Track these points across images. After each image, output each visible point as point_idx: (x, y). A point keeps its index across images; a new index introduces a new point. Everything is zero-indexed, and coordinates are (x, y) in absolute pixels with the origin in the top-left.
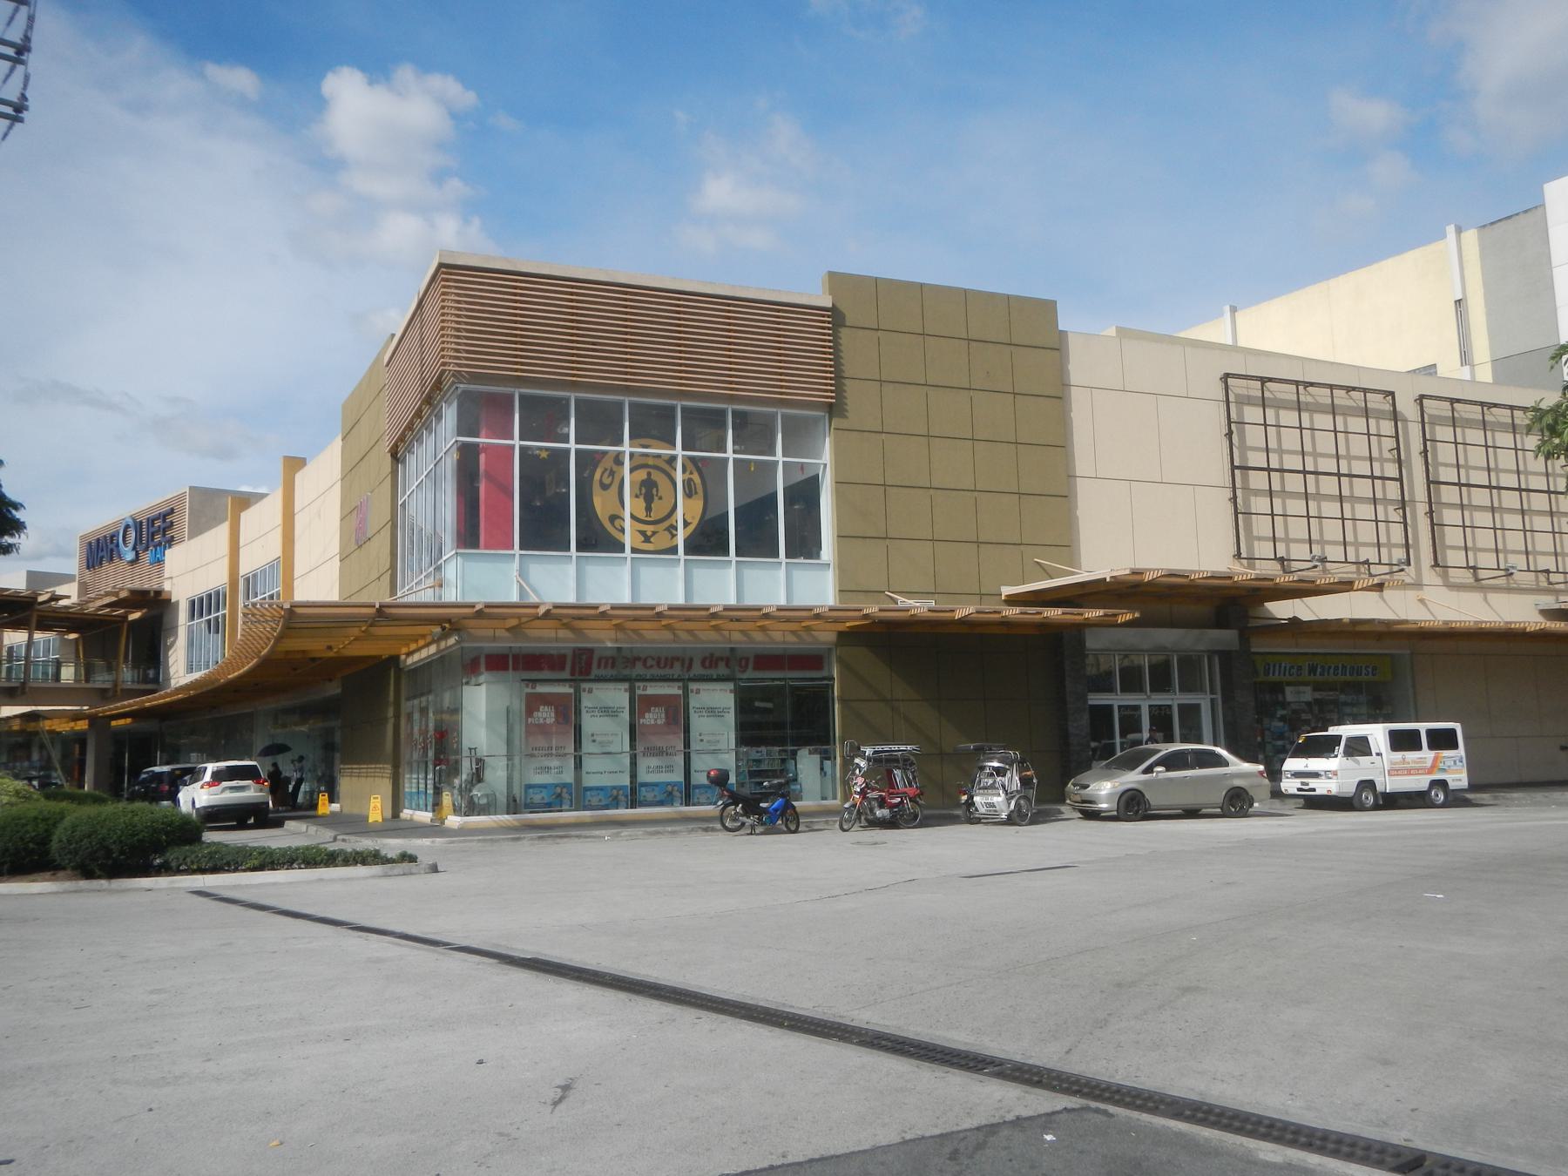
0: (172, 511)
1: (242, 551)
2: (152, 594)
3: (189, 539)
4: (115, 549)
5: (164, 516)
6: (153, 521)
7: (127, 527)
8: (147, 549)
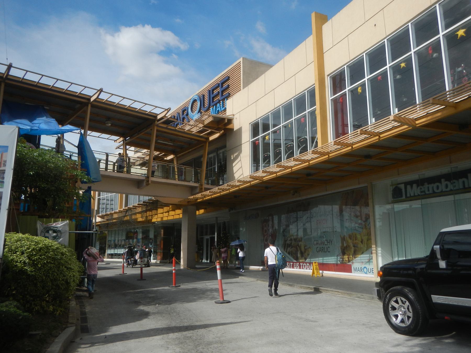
0: (228, 79)
1: (325, 55)
2: (226, 121)
3: (243, 89)
4: (186, 117)
5: (223, 84)
6: (213, 90)
7: (195, 101)
8: (208, 109)
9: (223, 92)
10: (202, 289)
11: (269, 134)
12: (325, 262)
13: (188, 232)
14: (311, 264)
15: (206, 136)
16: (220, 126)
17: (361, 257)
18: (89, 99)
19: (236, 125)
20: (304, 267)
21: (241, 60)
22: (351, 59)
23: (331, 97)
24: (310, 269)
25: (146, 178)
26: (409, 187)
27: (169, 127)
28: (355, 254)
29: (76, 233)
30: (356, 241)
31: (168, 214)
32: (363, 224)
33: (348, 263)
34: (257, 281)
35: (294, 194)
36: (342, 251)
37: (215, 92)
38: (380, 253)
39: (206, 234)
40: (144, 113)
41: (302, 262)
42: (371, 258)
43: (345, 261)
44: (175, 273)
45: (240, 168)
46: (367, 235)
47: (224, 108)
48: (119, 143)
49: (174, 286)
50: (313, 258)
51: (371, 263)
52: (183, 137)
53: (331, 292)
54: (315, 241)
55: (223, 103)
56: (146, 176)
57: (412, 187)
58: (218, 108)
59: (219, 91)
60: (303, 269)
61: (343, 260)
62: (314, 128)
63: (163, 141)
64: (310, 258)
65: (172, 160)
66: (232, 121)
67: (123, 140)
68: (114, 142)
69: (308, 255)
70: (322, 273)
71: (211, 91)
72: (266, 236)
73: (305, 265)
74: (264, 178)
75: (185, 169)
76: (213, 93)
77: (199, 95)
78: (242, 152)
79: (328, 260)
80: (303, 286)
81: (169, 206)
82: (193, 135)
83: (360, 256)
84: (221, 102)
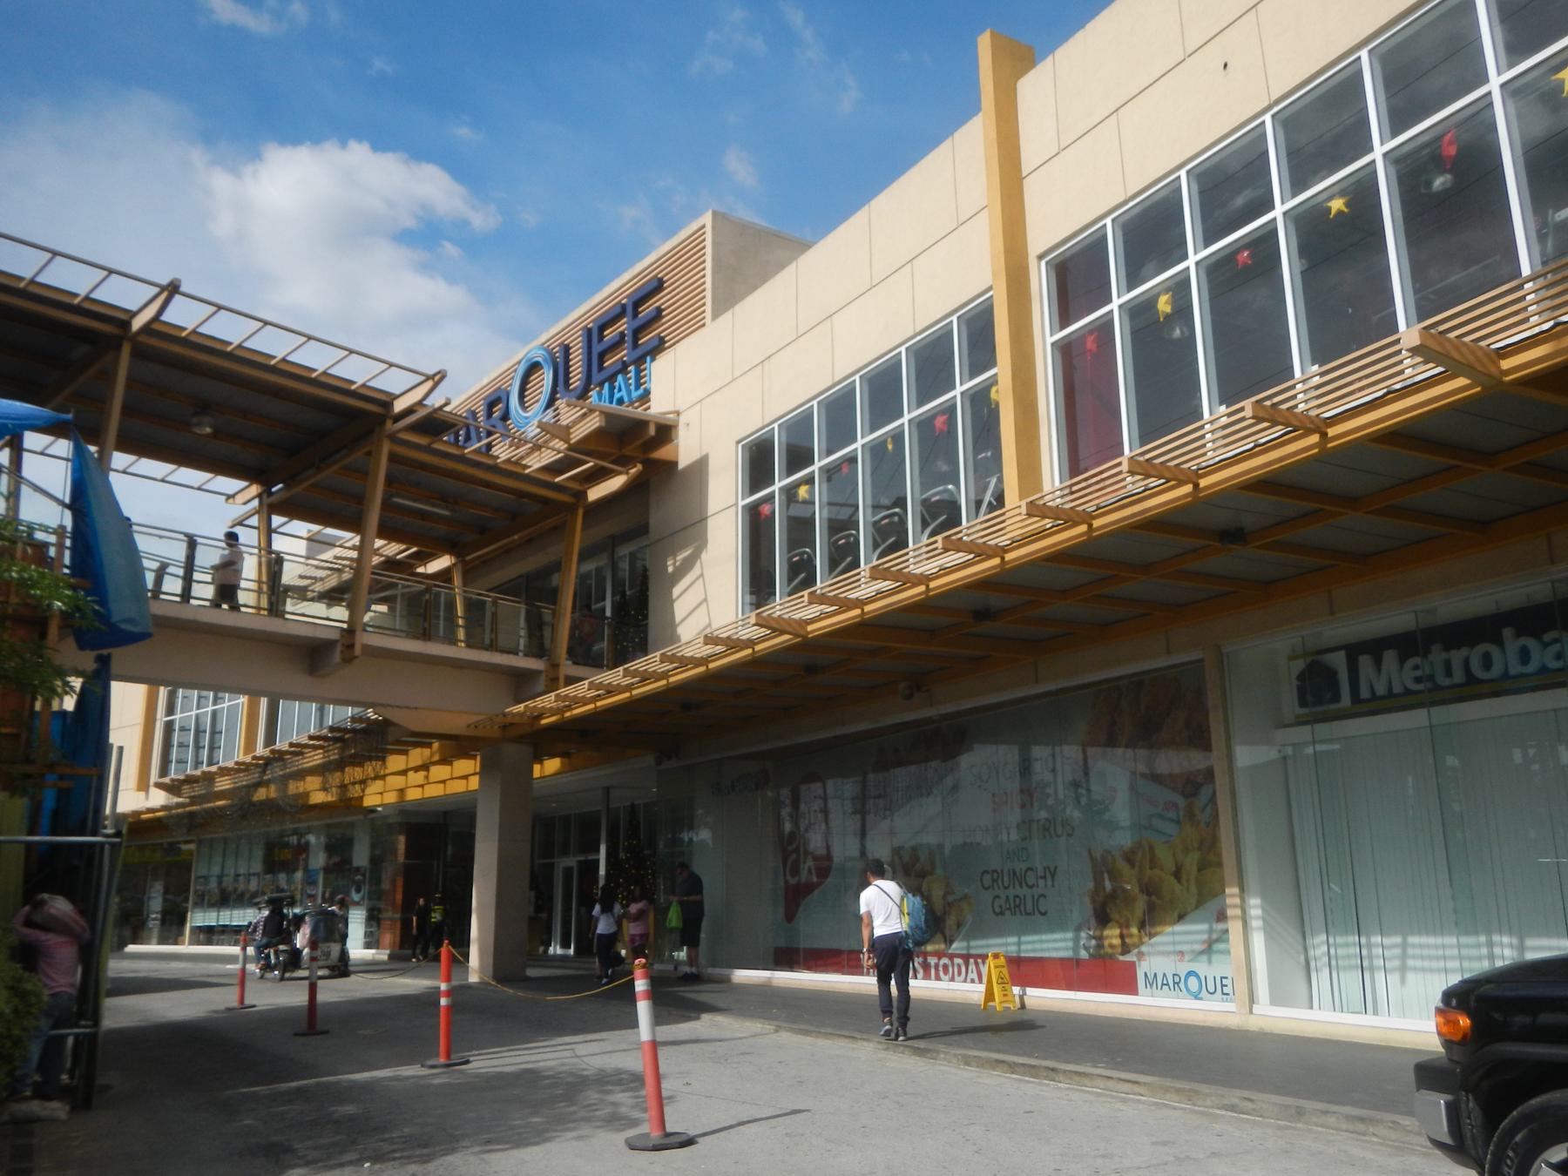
0: (658, 286)
2: (652, 431)
4: (500, 424)
5: (639, 302)
6: (602, 328)
7: (534, 367)
8: (583, 394)
9: (637, 332)
10: (560, 1073)
11: (809, 480)
12: (1027, 951)
13: (501, 840)
14: (972, 961)
15: (575, 486)
16: (627, 451)
17: (1173, 933)
18: (126, 325)
19: (685, 450)
20: (941, 969)
21: (707, 219)
22: (1130, 194)
23: (1051, 335)
24: (965, 981)
25: (342, 636)
26: (1365, 661)
27: (437, 446)
28: (1151, 920)
29: (29, 845)
30: (1157, 871)
31: (427, 777)
32: (1181, 802)
33: (1121, 958)
34: (776, 1031)
35: (910, 696)
36: (1095, 910)
37: (610, 334)
38: (1257, 918)
39: (565, 852)
40: (341, 388)
41: (934, 954)
42: (1215, 936)
43: (1109, 951)
44: (448, 1008)
45: (700, 604)
46: (1199, 849)
47: (641, 391)
48: (245, 503)
49: (442, 1060)
50: (975, 938)
51: (1215, 958)
52: (488, 485)
53: (1100, 1082)
54: (986, 872)
55: (638, 372)
56: (345, 626)
57: (1378, 663)
58: (620, 390)
59: (625, 330)
60: (938, 978)
61: (1100, 946)
62: (983, 455)
63: (415, 501)
64: (968, 938)
65: (445, 575)
66: (673, 431)
67: (259, 496)
68: (227, 499)
69: (959, 925)
70: (1021, 997)
71: (594, 334)
72: (794, 857)
73: (945, 967)
74: (810, 628)
75: (495, 603)
76: (601, 338)
77: (549, 346)
78: (709, 546)
79: (1038, 946)
80: (975, 1057)
81: (429, 745)
82: (528, 479)
83: (1169, 929)
84: (632, 368)
